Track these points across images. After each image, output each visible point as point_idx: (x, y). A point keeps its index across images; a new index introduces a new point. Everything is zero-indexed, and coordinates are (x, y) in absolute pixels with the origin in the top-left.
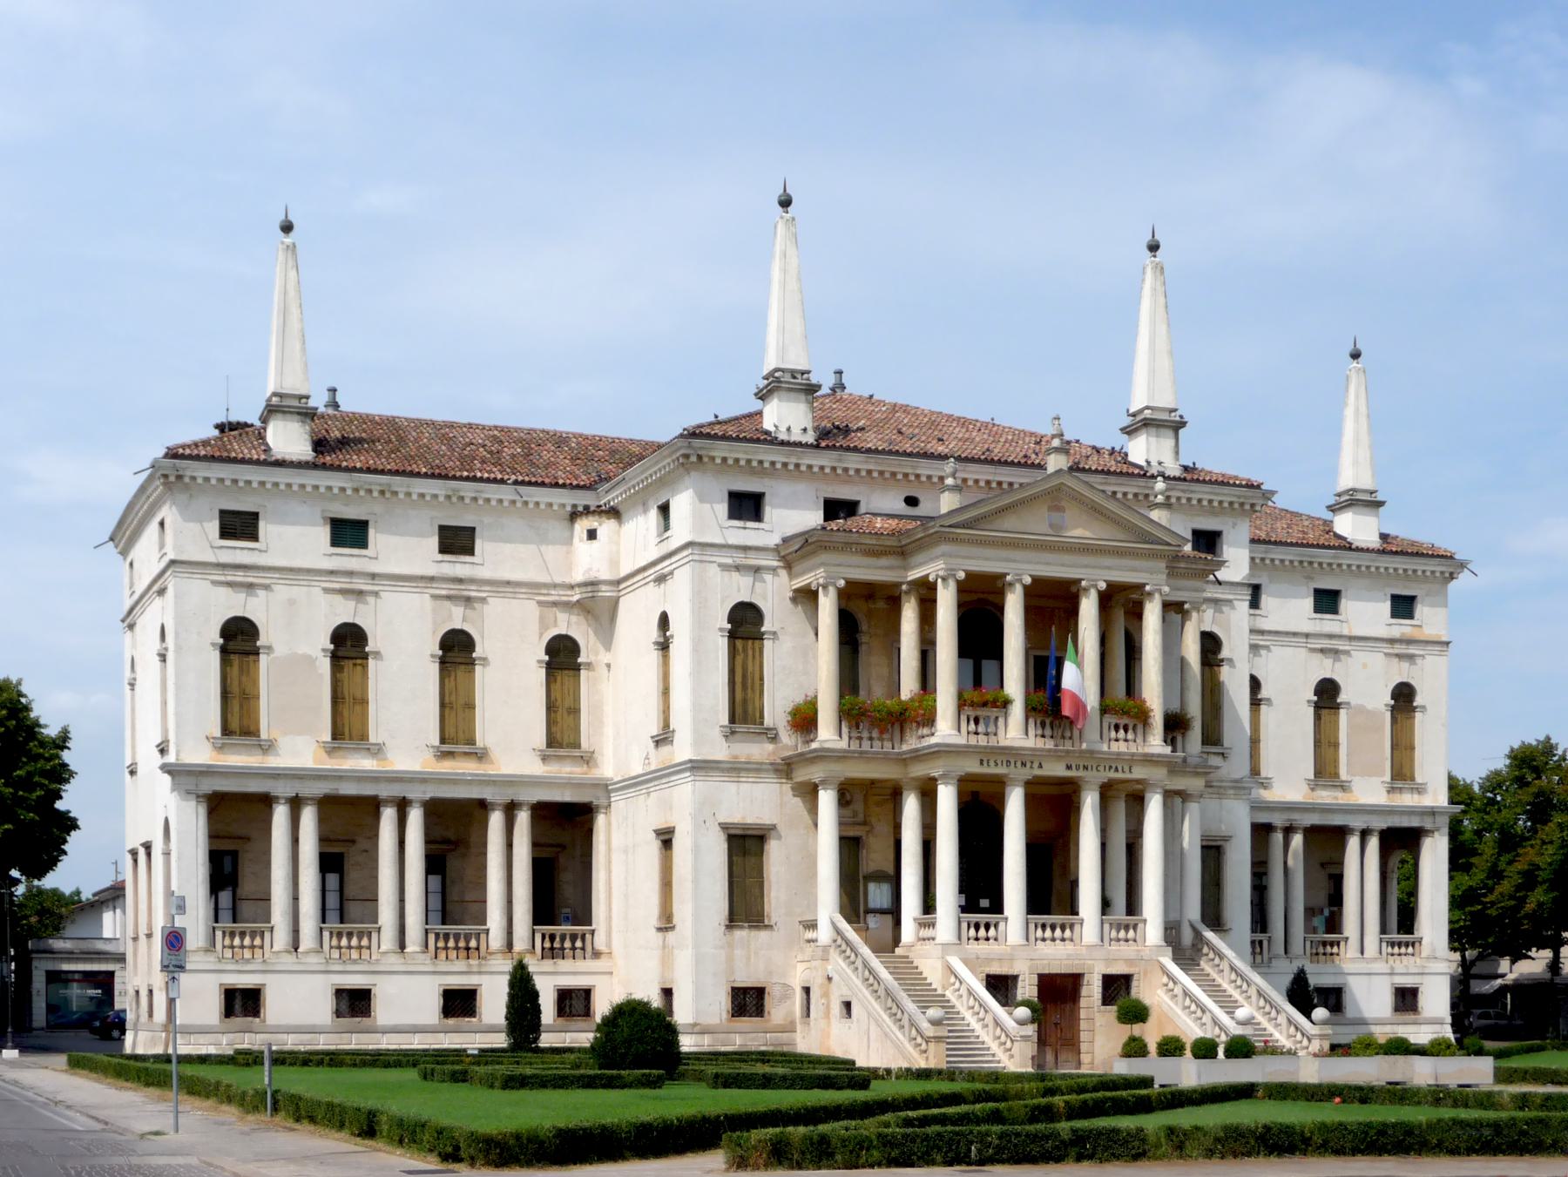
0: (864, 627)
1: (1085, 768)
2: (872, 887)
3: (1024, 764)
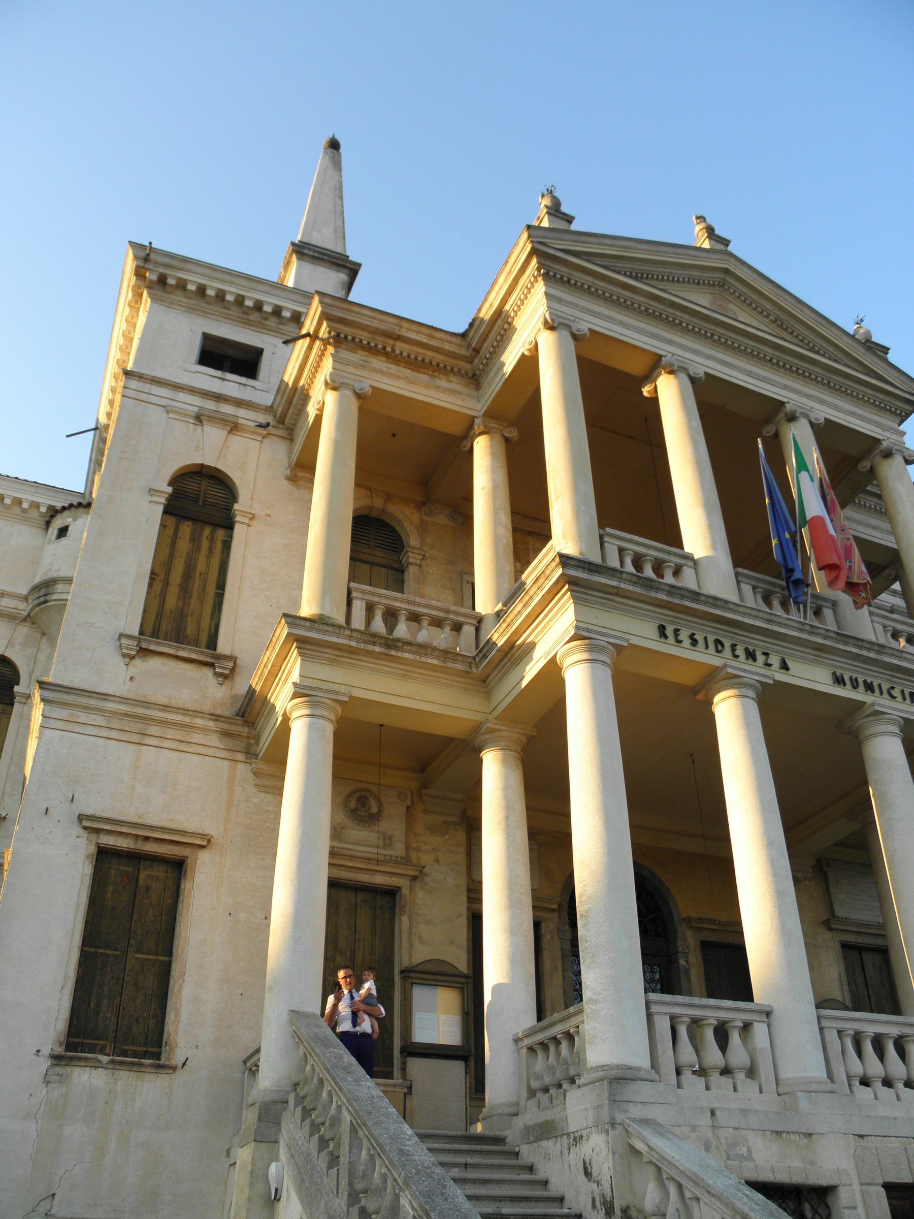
0: (413, 541)
1: (869, 687)
2: (419, 994)
3: (751, 655)
